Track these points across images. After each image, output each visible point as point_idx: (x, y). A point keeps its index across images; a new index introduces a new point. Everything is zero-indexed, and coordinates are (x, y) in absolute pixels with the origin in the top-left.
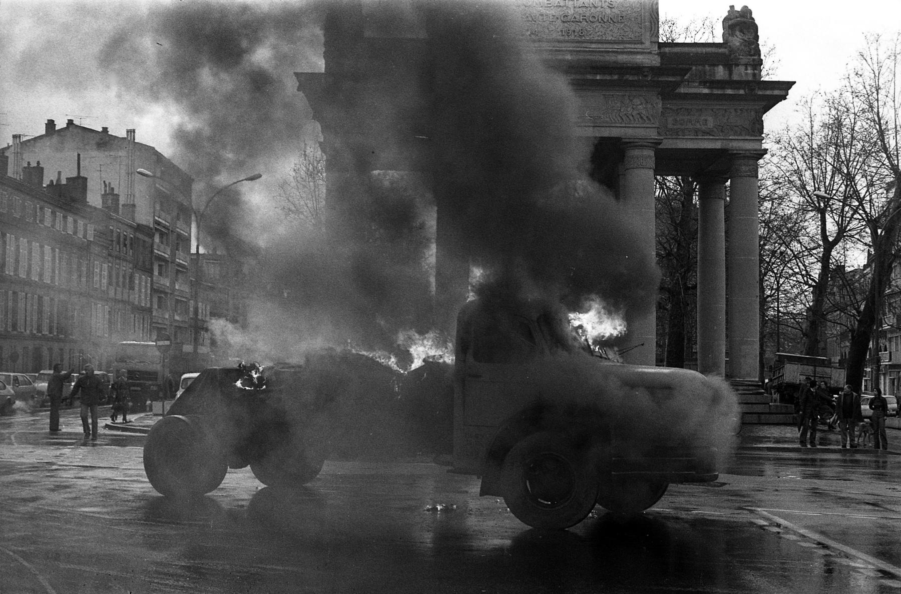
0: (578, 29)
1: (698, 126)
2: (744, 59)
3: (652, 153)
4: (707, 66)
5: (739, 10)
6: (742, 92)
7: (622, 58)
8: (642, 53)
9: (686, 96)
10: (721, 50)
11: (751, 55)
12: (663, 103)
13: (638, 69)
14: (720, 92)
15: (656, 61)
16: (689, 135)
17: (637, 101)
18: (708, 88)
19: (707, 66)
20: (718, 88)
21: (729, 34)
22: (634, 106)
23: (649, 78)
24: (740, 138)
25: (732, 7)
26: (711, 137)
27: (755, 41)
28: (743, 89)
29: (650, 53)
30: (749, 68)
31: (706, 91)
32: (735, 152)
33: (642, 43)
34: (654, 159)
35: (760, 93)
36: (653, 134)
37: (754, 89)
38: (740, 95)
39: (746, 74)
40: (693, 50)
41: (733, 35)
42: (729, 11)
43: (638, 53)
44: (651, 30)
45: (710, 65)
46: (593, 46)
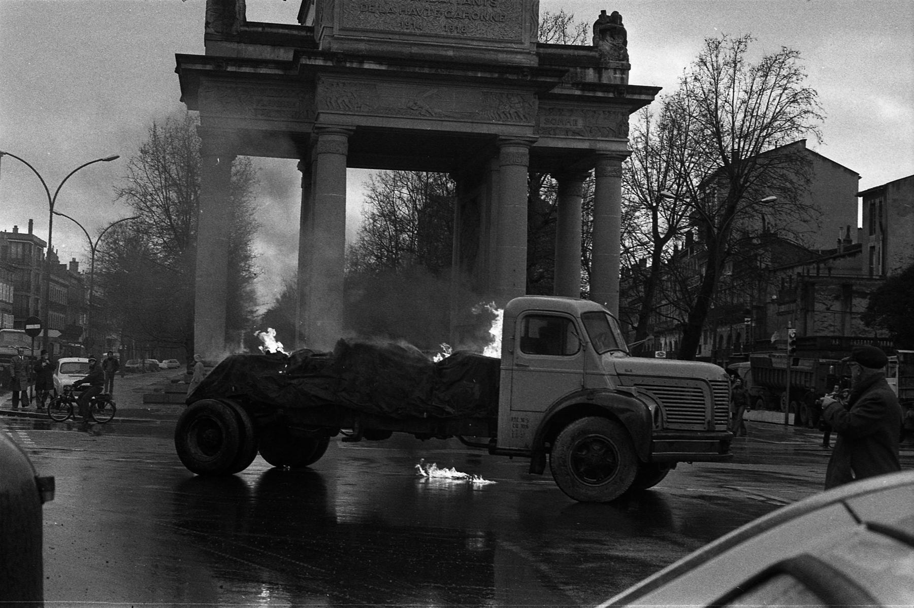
1: (568, 126)
7: (502, 57)
8: (521, 53)
13: (518, 69)
15: (533, 62)
17: (515, 100)
20: (589, 91)
21: (599, 38)
23: (529, 78)
25: (604, 12)
29: (529, 53)
31: (578, 92)
33: (522, 43)
34: (528, 157)
35: (628, 97)
41: (603, 39)
43: (517, 53)
44: (531, 30)
45: (581, 68)
46: (475, 43)
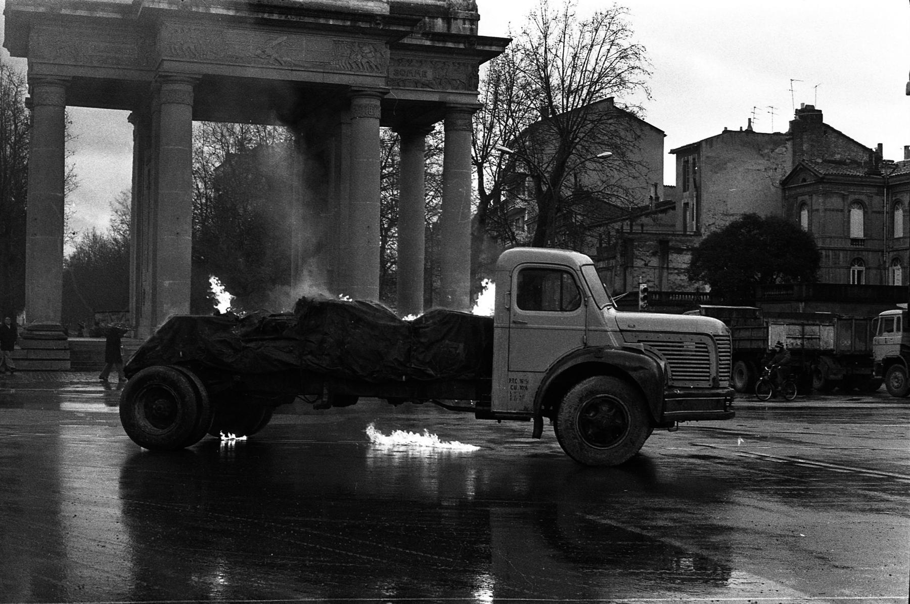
1: (418, 77)
11: (469, 11)
12: (391, 54)
13: (369, 16)
14: (441, 45)
17: (366, 50)
18: (430, 40)
20: (439, 41)
23: (381, 27)
26: (431, 90)
30: (467, 22)
31: (428, 43)
32: (452, 105)
36: (381, 84)
39: (464, 28)
45: (430, 17)
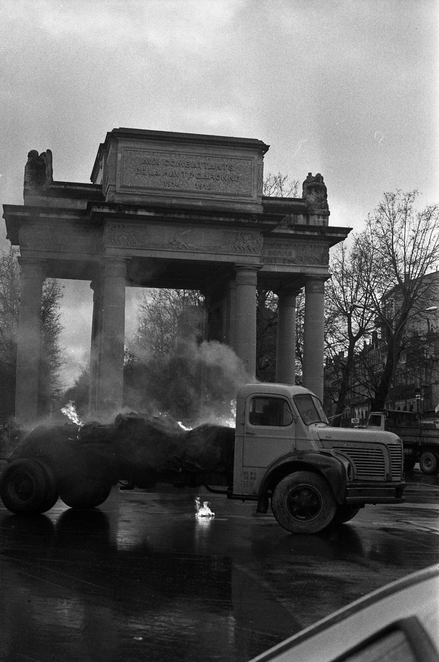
0: (207, 184)
1: (285, 256)
2: (317, 211)
3: (255, 274)
4: (292, 214)
5: (315, 176)
6: (316, 234)
7: (238, 206)
8: (251, 204)
9: (278, 235)
10: (302, 204)
13: (248, 215)
15: (259, 210)
16: (280, 262)
17: (247, 238)
18: (294, 230)
19: (292, 214)
20: (299, 230)
21: (307, 193)
22: (245, 241)
23: (256, 222)
24: (314, 266)
25: (310, 174)
27: (325, 199)
28: (317, 232)
29: (257, 204)
30: (320, 217)
31: (292, 232)
33: (251, 197)
35: (328, 235)
37: (325, 233)
38: (314, 236)
39: (318, 221)
40: (284, 203)
41: (310, 193)
42: (307, 177)
43: (248, 203)
44: (257, 188)
45: (294, 214)
46: (218, 197)
